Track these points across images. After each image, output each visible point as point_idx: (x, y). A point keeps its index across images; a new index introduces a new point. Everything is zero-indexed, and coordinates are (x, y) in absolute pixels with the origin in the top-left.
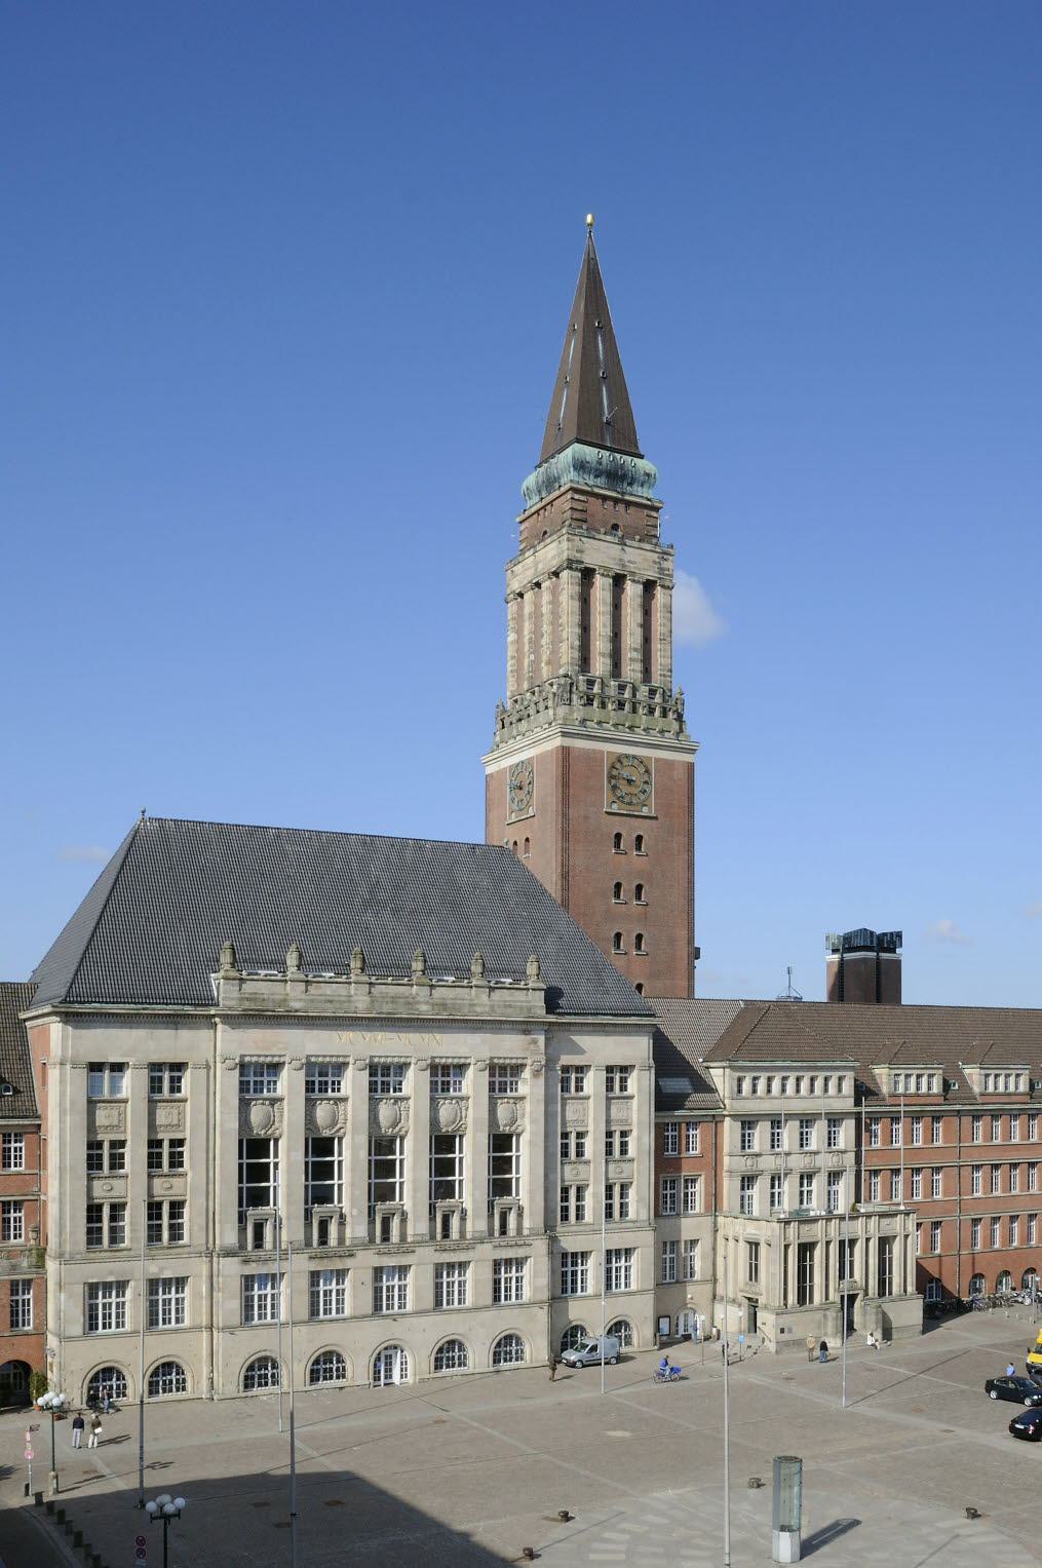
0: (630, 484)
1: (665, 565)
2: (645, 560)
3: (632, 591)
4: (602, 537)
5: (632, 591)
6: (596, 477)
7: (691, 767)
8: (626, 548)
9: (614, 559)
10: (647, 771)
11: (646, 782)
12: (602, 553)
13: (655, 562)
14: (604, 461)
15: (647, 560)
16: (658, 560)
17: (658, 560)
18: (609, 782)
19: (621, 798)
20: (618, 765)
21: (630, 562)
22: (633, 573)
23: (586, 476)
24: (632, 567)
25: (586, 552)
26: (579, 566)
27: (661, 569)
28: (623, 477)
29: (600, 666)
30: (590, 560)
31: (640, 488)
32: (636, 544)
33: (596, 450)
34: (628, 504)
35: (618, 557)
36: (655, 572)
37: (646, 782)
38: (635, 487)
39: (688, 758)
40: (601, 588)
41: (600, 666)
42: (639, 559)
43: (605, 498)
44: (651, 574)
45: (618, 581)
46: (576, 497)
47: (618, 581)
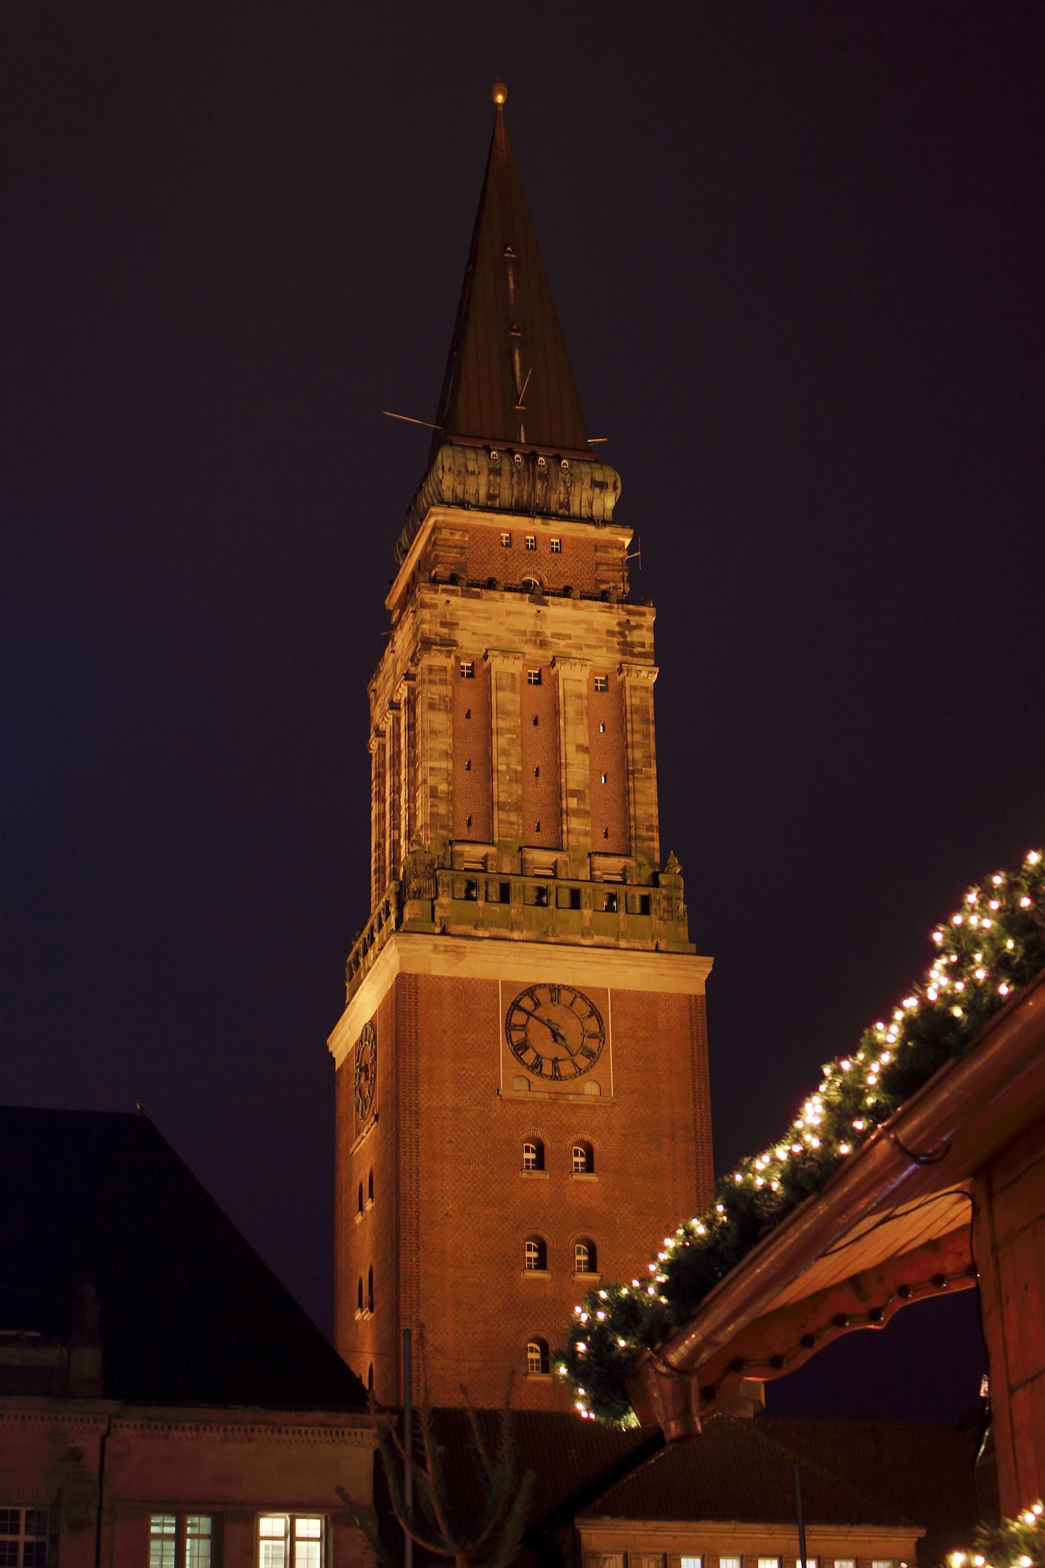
2: (590, 629)
9: (523, 633)
10: (594, 1012)
11: (593, 1036)
13: (611, 633)
15: (596, 631)
16: (617, 629)
17: (617, 629)
18: (509, 1038)
21: (554, 635)
25: (461, 626)
35: (530, 629)
36: (610, 649)
37: (593, 1036)
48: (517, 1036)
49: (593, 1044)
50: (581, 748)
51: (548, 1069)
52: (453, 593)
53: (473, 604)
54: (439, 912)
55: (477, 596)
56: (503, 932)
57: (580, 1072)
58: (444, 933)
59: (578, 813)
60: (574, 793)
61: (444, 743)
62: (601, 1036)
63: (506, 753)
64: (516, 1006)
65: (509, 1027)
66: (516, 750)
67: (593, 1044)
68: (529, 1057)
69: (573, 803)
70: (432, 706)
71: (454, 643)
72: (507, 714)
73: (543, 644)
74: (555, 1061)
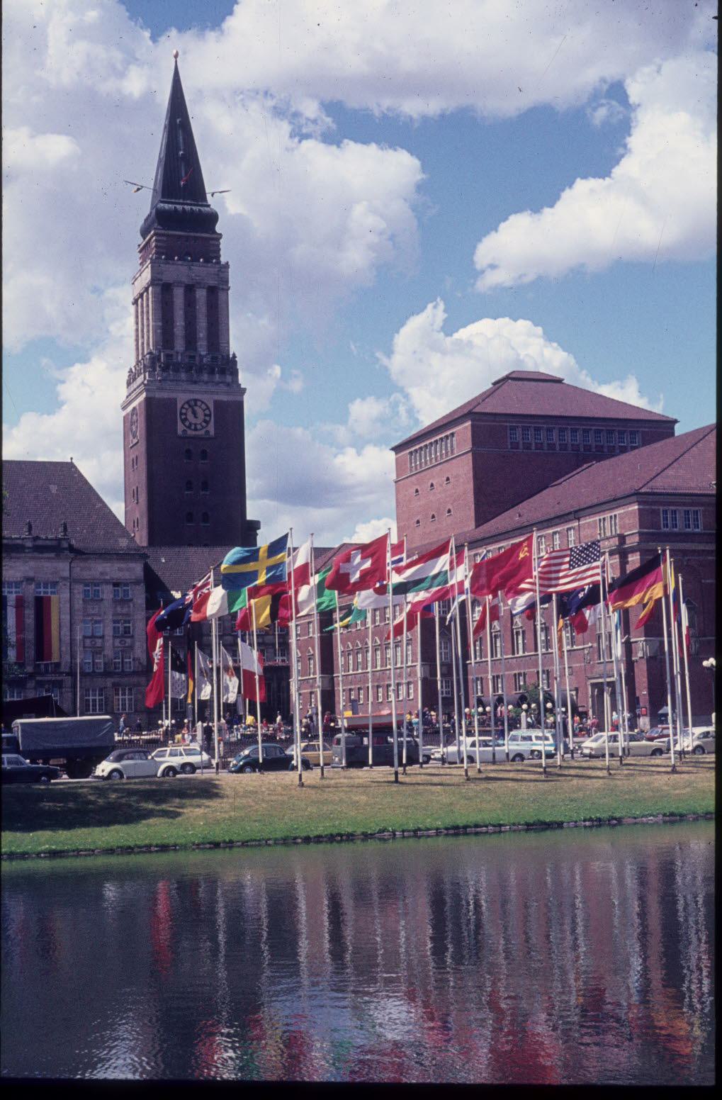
1: (221, 275)
3: (201, 294)
5: (201, 294)
7: (240, 405)
10: (208, 408)
19: (189, 427)
20: (186, 406)
22: (199, 283)
26: (160, 282)
29: (179, 345)
39: (238, 399)
40: (179, 295)
41: (179, 345)
44: (212, 283)
45: (190, 289)
47: (190, 289)
48: (183, 417)
49: (207, 418)
51: (193, 427)
57: (203, 427)
62: (210, 415)
64: (182, 407)
65: (181, 414)
67: (207, 418)
68: (187, 424)
71: (161, 280)
74: (195, 424)
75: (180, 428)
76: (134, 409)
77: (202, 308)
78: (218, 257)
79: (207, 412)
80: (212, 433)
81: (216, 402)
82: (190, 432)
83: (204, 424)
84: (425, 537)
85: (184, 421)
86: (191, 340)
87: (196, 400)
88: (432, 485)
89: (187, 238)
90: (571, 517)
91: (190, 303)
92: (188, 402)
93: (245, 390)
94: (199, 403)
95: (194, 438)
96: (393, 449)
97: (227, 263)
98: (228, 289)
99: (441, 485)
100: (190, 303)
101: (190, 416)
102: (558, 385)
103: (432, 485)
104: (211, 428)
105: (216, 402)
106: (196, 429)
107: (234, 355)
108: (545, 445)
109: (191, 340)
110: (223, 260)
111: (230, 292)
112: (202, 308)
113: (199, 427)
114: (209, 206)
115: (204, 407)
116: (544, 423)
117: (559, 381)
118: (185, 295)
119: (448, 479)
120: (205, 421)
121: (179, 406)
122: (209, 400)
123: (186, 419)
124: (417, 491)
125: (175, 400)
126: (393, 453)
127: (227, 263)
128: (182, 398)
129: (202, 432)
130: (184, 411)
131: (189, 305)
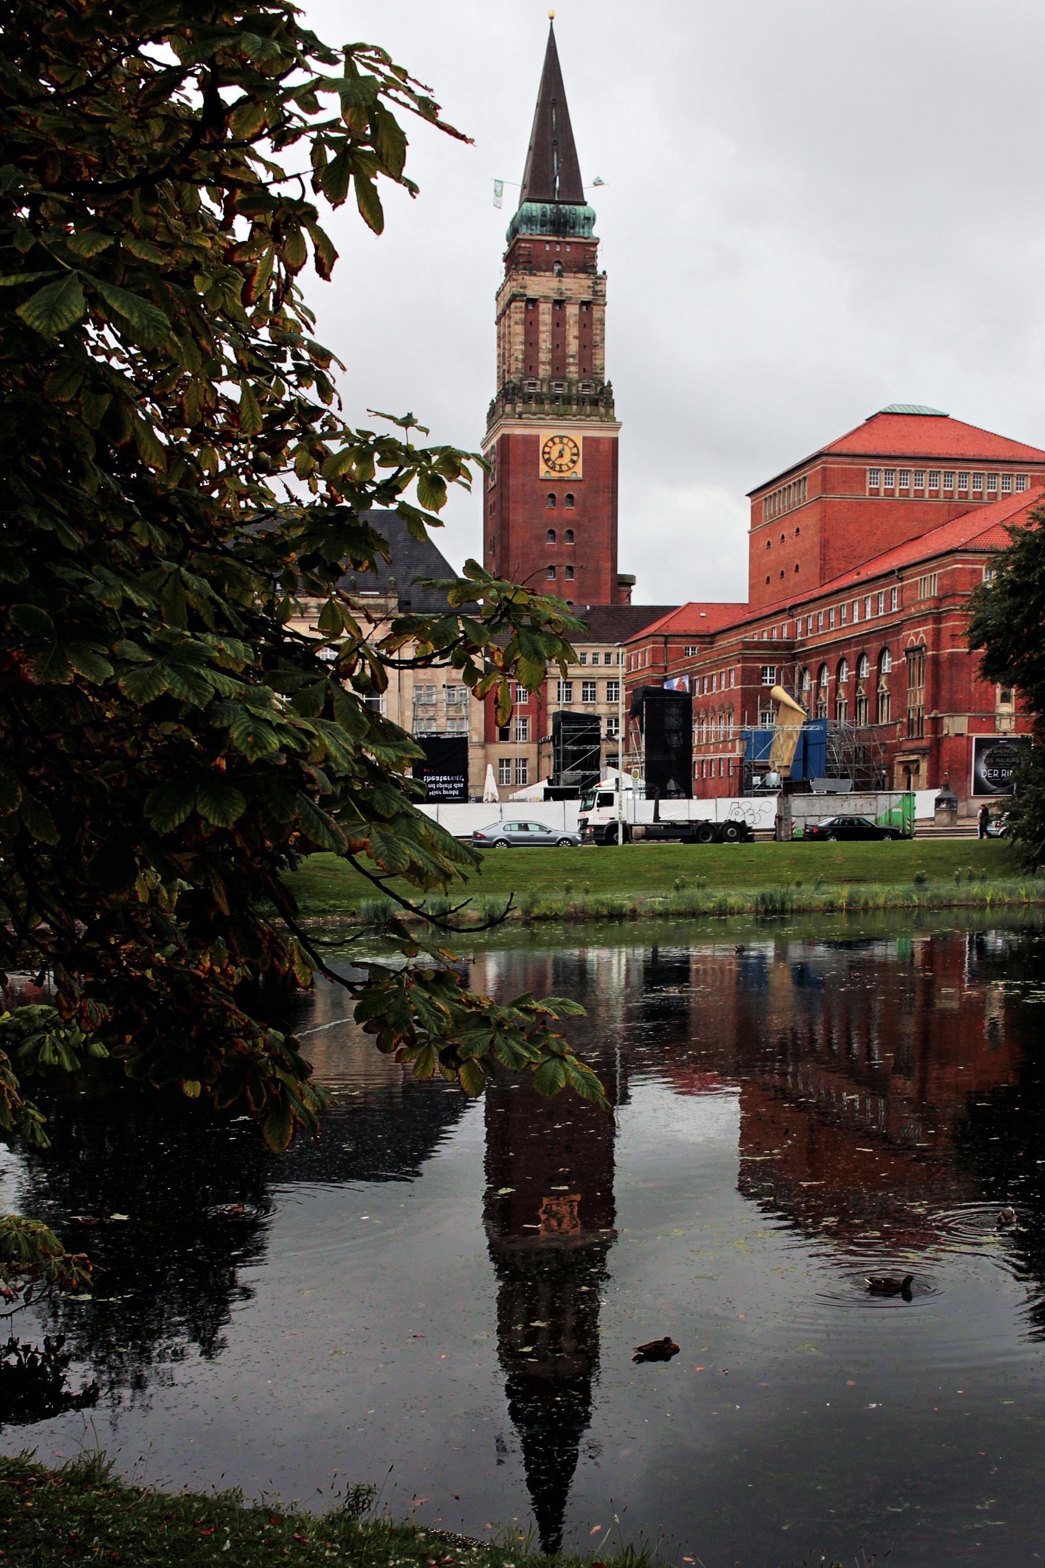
0: (573, 228)
1: (598, 288)
3: (572, 311)
4: (542, 274)
5: (572, 311)
6: (542, 226)
7: (615, 441)
8: (564, 279)
10: (576, 446)
11: (575, 455)
12: (540, 285)
13: (589, 287)
14: (549, 213)
19: (553, 468)
20: (550, 444)
22: (570, 298)
23: (534, 227)
24: (569, 294)
27: (595, 293)
28: (566, 223)
30: (530, 293)
31: (581, 230)
32: (572, 275)
33: (539, 205)
34: (569, 243)
37: (575, 455)
38: (577, 230)
39: (612, 434)
40: (545, 315)
41: (544, 371)
42: (575, 287)
43: (548, 242)
44: (587, 297)
45: (559, 303)
46: (523, 245)
47: (559, 303)
48: (546, 456)
49: (575, 458)
50: (575, 337)
51: (557, 468)
52: (525, 274)
53: (533, 278)
54: (518, 410)
55: (535, 275)
56: (542, 416)
57: (570, 469)
58: (520, 418)
59: (573, 364)
60: (572, 356)
61: (521, 338)
62: (577, 455)
63: (545, 341)
64: (546, 445)
65: (544, 453)
66: (549, 340)
67: (575, 458)
69: (571, 360)
70: (516, 323)
72: (546, 324)
73: (561, 294)
75: (543, 468)
76: (493, 447)
77: (573, 331)
78: (594, 267)
79: (575, 451)
80: (580, 476)
81: (585, 439)
82: (555, 475)
83: (571, 465)
84: (777, 597)
85: (547, 461)
86: (559, 363)
87: (561, 437)
88: (783, 537)
89: (558, 243)
90: (894, 577)
91: (559, 323)
92: (552, 440)
93: (620, 424)
94: (565, 441)
95: (560, 480)
96: (748, 495)
97: (604, 273)
98: (605, 305)
99: (791, 538)
100: (559, 323)
101: (554, 455)
102: (943, 420)
103: (783, 537)
104: (578, 471)
105: (585, 439)
106: (561, 471)
107: (609, 383)
108: (942, 493)
109: (559, 363)
110: (600, 270)
111: (606, 308)
112: (573, 331)
113: (564, 468)
114: (585, 204)
115: (571, 445)
116: (910, 466)
117: (946, 417)
118: (554, 314)
119: (798, 530)
120: (574, 462)
121: (542, 443)
122: (578, 436)
123: (549, 460)
124: (769, 543)
125: (538, 437)
126: (749, 499)
127: (604, 273)
128: (545, 436)
129: (566, 475)
130: (547, 450)
131: (558, 325)
